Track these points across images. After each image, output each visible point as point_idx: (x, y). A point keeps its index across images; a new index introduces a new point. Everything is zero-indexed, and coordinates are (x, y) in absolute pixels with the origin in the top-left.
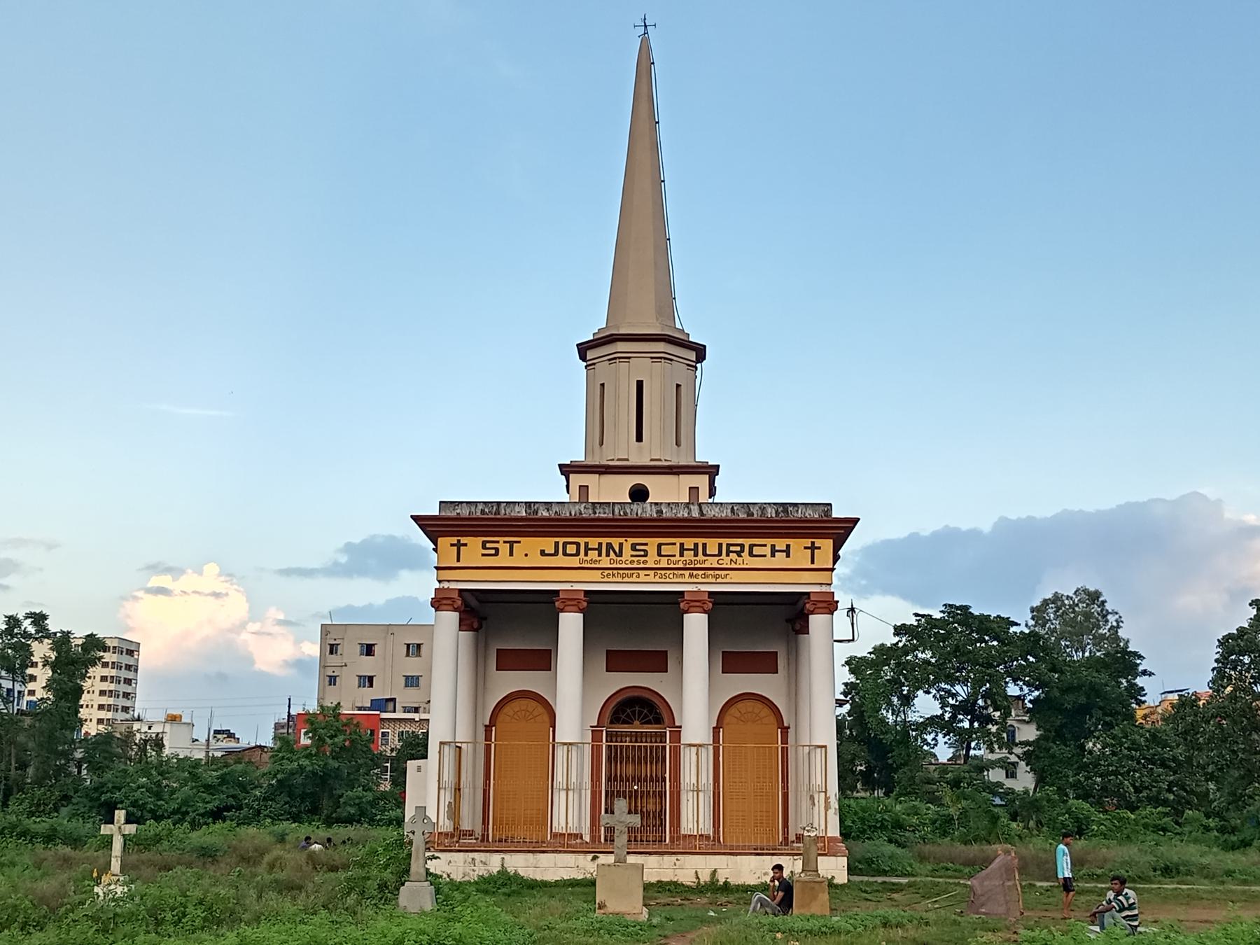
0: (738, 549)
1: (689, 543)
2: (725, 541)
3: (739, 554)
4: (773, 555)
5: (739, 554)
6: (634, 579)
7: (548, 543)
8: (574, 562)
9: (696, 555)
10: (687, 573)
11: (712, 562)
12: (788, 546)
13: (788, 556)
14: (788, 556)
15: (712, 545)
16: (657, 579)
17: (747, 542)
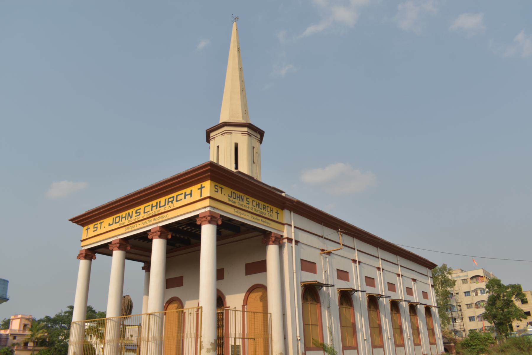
0: (172, 199)
1: (154, 203)
2: (167, 197)
3: (172, 202)
4: (185, 198)
5: (172, 202)
6: (135, 228)
7: (110, 220)
8: (117, 226)
9: (157, 208)
10: (152, 219)
11: (162, 210)
12: (191, 191)
13: (191, 196)
14: (191, 196)
15: (162, 200)
16: (143, 226)
17: (174, 195)
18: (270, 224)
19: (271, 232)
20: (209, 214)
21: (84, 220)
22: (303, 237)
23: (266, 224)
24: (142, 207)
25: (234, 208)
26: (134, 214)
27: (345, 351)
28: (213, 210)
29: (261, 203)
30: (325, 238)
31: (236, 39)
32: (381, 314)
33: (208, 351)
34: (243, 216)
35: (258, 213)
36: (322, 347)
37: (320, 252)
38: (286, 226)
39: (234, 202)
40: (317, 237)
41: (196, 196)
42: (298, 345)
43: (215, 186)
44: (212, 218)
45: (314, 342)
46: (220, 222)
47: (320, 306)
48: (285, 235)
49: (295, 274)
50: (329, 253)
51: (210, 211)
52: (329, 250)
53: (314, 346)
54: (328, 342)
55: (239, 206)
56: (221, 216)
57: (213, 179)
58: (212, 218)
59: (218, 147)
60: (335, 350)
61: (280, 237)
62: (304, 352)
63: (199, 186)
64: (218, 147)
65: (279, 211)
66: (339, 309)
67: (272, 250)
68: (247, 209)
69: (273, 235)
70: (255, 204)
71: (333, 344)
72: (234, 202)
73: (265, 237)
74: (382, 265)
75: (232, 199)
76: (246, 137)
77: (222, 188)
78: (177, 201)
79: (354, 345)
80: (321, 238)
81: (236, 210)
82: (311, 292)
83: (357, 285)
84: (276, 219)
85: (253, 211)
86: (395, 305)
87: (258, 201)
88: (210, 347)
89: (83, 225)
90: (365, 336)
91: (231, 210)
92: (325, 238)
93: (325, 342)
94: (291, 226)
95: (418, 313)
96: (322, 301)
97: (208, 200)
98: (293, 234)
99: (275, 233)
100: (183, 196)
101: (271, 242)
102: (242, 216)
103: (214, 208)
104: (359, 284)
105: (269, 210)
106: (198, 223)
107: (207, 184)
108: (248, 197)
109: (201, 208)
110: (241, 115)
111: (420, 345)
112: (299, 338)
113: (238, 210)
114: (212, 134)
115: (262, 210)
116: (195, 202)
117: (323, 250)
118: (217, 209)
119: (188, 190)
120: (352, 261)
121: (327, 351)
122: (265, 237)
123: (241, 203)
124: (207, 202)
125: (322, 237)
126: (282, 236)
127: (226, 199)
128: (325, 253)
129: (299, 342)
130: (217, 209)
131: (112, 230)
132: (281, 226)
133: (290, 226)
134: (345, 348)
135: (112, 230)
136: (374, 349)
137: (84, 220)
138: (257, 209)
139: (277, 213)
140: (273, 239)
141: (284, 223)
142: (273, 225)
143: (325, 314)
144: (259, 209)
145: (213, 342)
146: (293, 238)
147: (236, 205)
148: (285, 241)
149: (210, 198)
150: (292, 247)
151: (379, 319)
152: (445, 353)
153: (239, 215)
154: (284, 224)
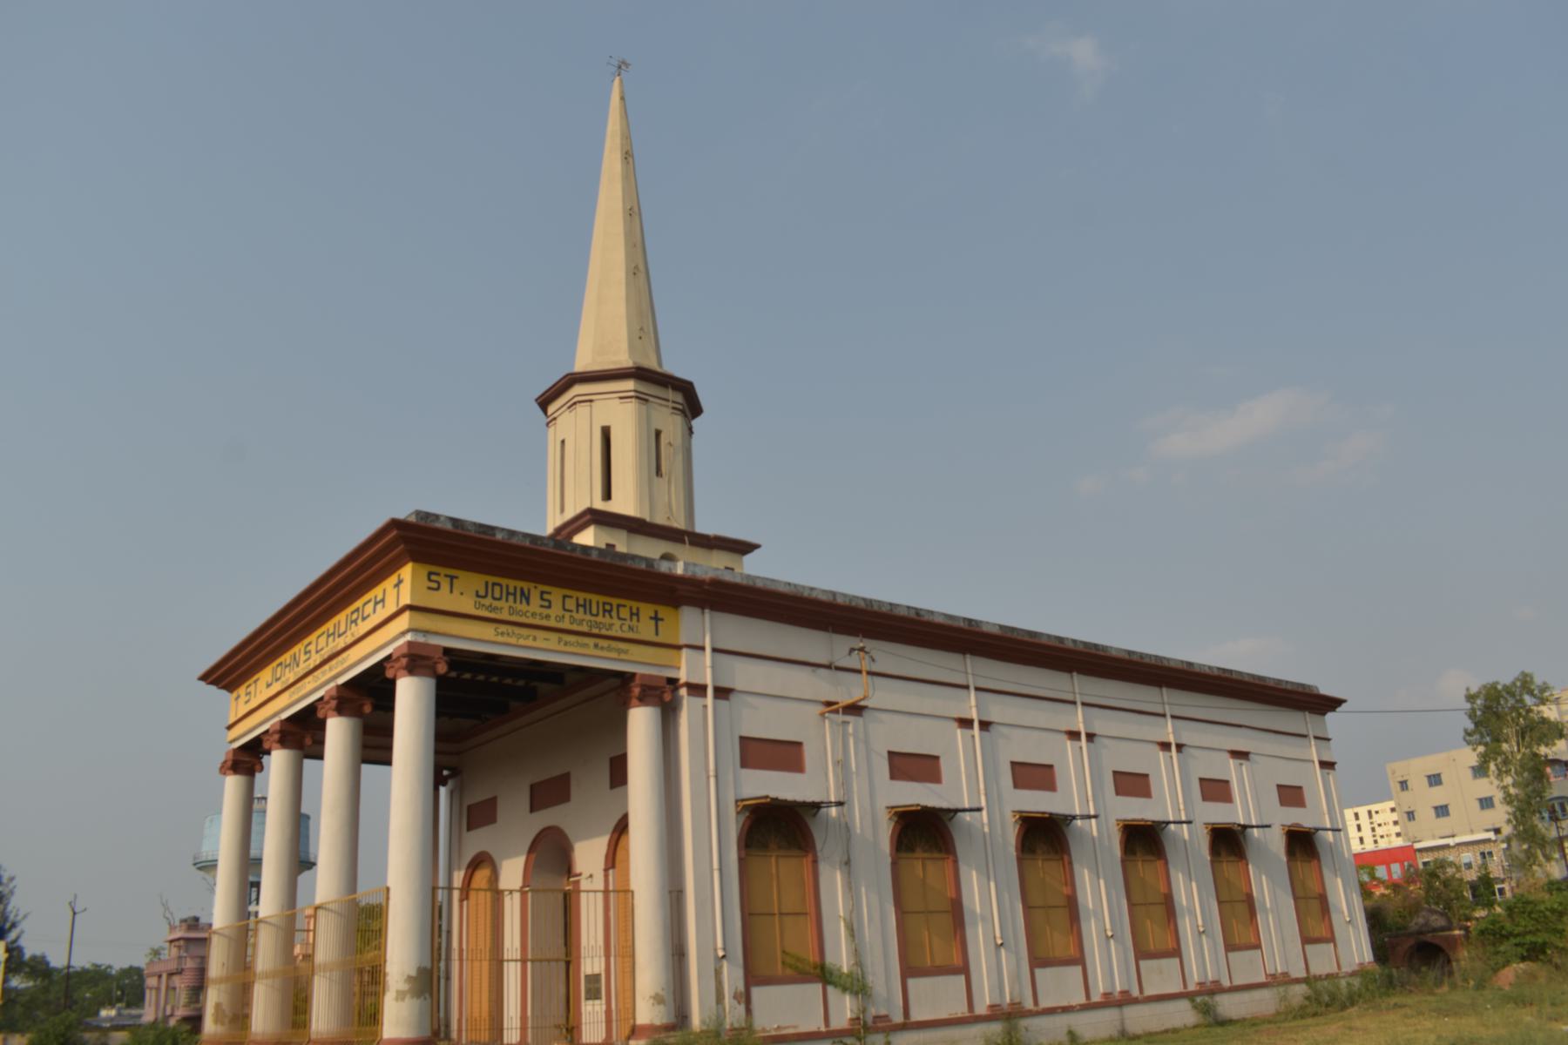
3: (355, 621)
10: (326, 667)
15: (341, 617)
18: (626, 652)
19: (634, 675)
20: (405, 651)
21: (230, 673)
22: (744, 675)
23: (614, 655)
24: (313, 637)
25: (494, 625)
26: (303, 657)
27: (911, 982)
28: (421, 639)
29: (595, 598)
30: (838, 669)
31: (618, 127)
32: (1076, 867)
33: (401, 996)
34: (530, 642)
35: (585, 628)
36: (823, 975)
37: (821, 708)
38: (685, 652)
39: (495, 609)
40: (809, 669)
41: (391, 608)
42: (718, 973)
43: (430, 574)
44: (416, 660)
45: (789, 960)
46: (442, 668)
47: (815, 862)
48: (683, 676)
49: (712, 780)
50: (855, 709)
51: (410, 643)
52: (848, 701)
53: (789, 972)
54: (840, 957)
55: (514, 618)
56: (447, 651)
57: (418, 558)
58: (416, 660)
59: (563, 442)
60: (870, 979)
61: (664, 683)
62: (741, 986)
63: (393, 579)
64: (563, 442)
65: (664, 611)
66: (894, 864)
67: (641, 722)
68: (544, 623)
69: (638, 681)
70: (571, 604)
71: (859, 963)
72: (495, 609)
73: (618, 690)
74: (1085, 722)
75: (488, 601)
76: (631, 407)
77: (452, 578)
78: (364, 619)
79: (957, 961)
80: (822, 671)
81: (503, 628)
82: (777, 830)
83: (973, 790)
84: (652, 637)
85: (566, 625)
86: (1143, 840)
87: (582, 596)
88: (404, 987)
89: (231, 687)
90: (1108, 926)
91: (487, 631)
92: (838, 669)
93: (830, 959)
94: (702, 648)
95: (1251, 853)
96: (819, 846)
97: (406, 615)
98: (709, 672)
99: (643, 676)
100: (371, 605)
101: (634, 701)
102: (522, 642)
103: (426, 632)
104: (982, 786)
105: (625, 613)
106: (389, 674)
107: (407, 571)
108: (546, 588)
109: (392, 639)
110: (624, 345)
111: (1258, 946)
112: (721, 953)
113: (510, 629)
114: (551, 409)
115: (600, 619)
116: (381, 624)
117: (829, 704)
118: (436, 633)
119: (377, 592)
120: (955, 725)
121: (835, 985)
122: (618, 690)
123: (524, 607)
124: (404, 622)
125: (828, 667)
126: (673, 682)
127: (467, 605)
128: (836, 711)
129: (725, 963)
130: (436, 633)
131: (272, 696)
132: (673, 652)
133: (697, 648)
134: (910, 970)
135: (272, 696)
136: (1038, 972)
137: (230, 673)
138: (580, 615)
139: (656, 619)
140: (637, 691)
141: (682, 641)
142: (637, 652)
143: (833, 883)
144: (588, 617)
145: (413, 973)
146: (709, 682)
147: (505, 616)
148: (683, 691)
149: (410, 607)
150: (705, 707)
151: (1070, 881)
152: (1377, 968)
153: (513, 640)
154: (679, 648)
